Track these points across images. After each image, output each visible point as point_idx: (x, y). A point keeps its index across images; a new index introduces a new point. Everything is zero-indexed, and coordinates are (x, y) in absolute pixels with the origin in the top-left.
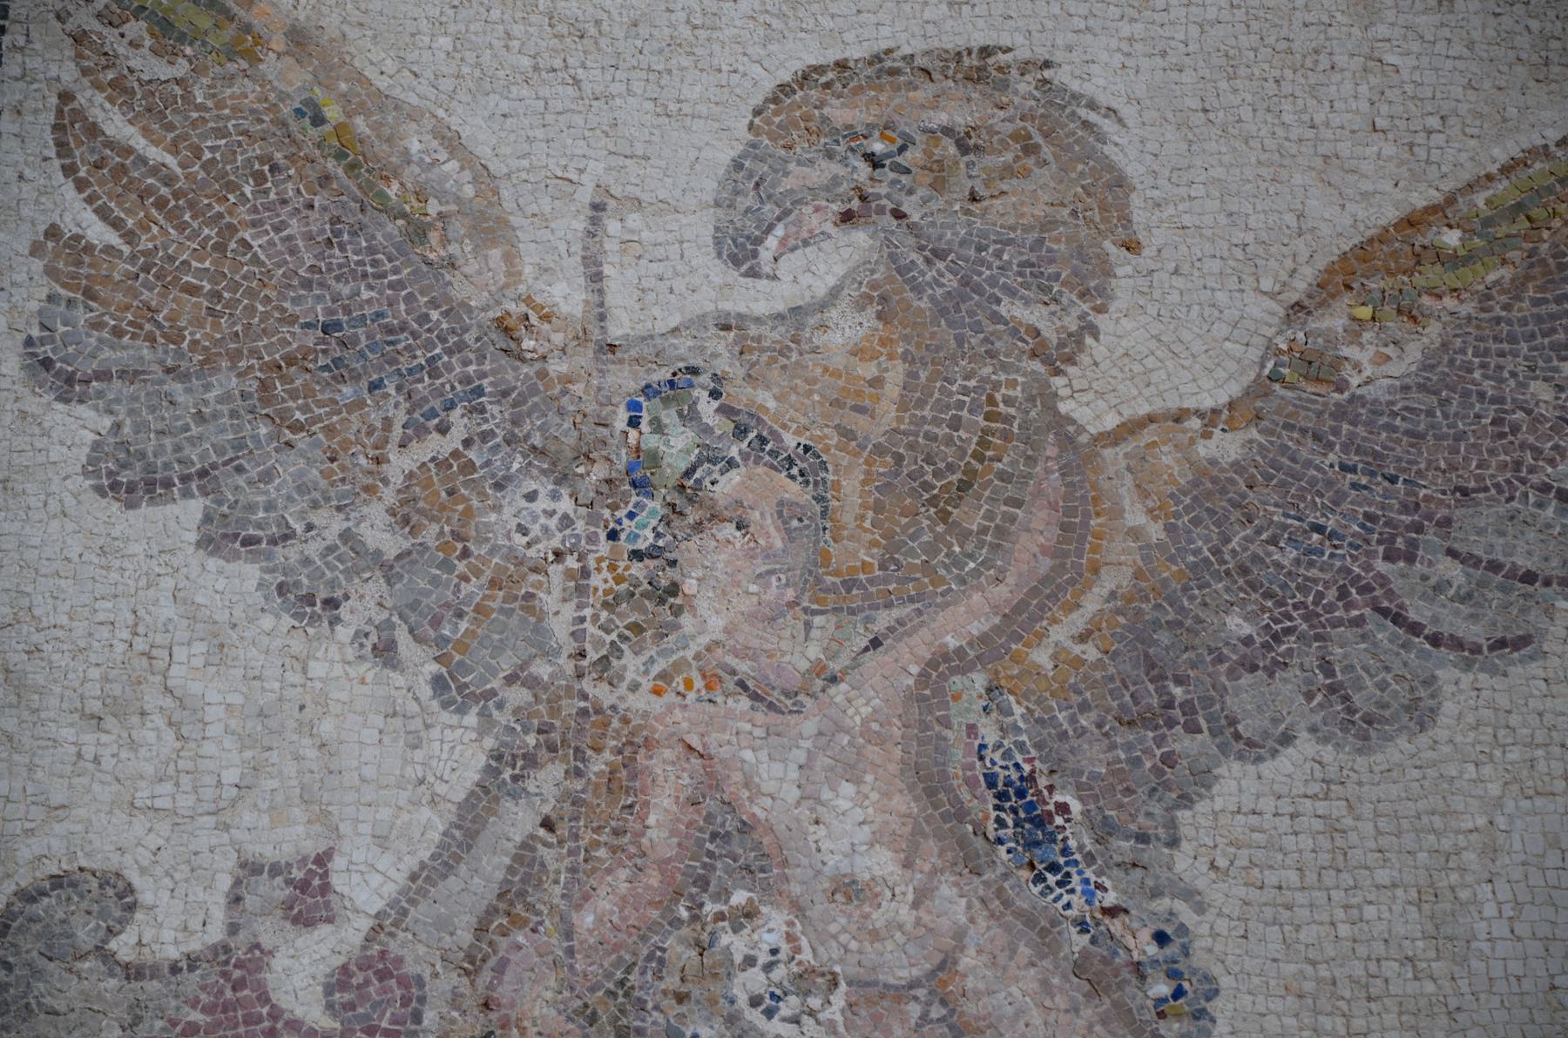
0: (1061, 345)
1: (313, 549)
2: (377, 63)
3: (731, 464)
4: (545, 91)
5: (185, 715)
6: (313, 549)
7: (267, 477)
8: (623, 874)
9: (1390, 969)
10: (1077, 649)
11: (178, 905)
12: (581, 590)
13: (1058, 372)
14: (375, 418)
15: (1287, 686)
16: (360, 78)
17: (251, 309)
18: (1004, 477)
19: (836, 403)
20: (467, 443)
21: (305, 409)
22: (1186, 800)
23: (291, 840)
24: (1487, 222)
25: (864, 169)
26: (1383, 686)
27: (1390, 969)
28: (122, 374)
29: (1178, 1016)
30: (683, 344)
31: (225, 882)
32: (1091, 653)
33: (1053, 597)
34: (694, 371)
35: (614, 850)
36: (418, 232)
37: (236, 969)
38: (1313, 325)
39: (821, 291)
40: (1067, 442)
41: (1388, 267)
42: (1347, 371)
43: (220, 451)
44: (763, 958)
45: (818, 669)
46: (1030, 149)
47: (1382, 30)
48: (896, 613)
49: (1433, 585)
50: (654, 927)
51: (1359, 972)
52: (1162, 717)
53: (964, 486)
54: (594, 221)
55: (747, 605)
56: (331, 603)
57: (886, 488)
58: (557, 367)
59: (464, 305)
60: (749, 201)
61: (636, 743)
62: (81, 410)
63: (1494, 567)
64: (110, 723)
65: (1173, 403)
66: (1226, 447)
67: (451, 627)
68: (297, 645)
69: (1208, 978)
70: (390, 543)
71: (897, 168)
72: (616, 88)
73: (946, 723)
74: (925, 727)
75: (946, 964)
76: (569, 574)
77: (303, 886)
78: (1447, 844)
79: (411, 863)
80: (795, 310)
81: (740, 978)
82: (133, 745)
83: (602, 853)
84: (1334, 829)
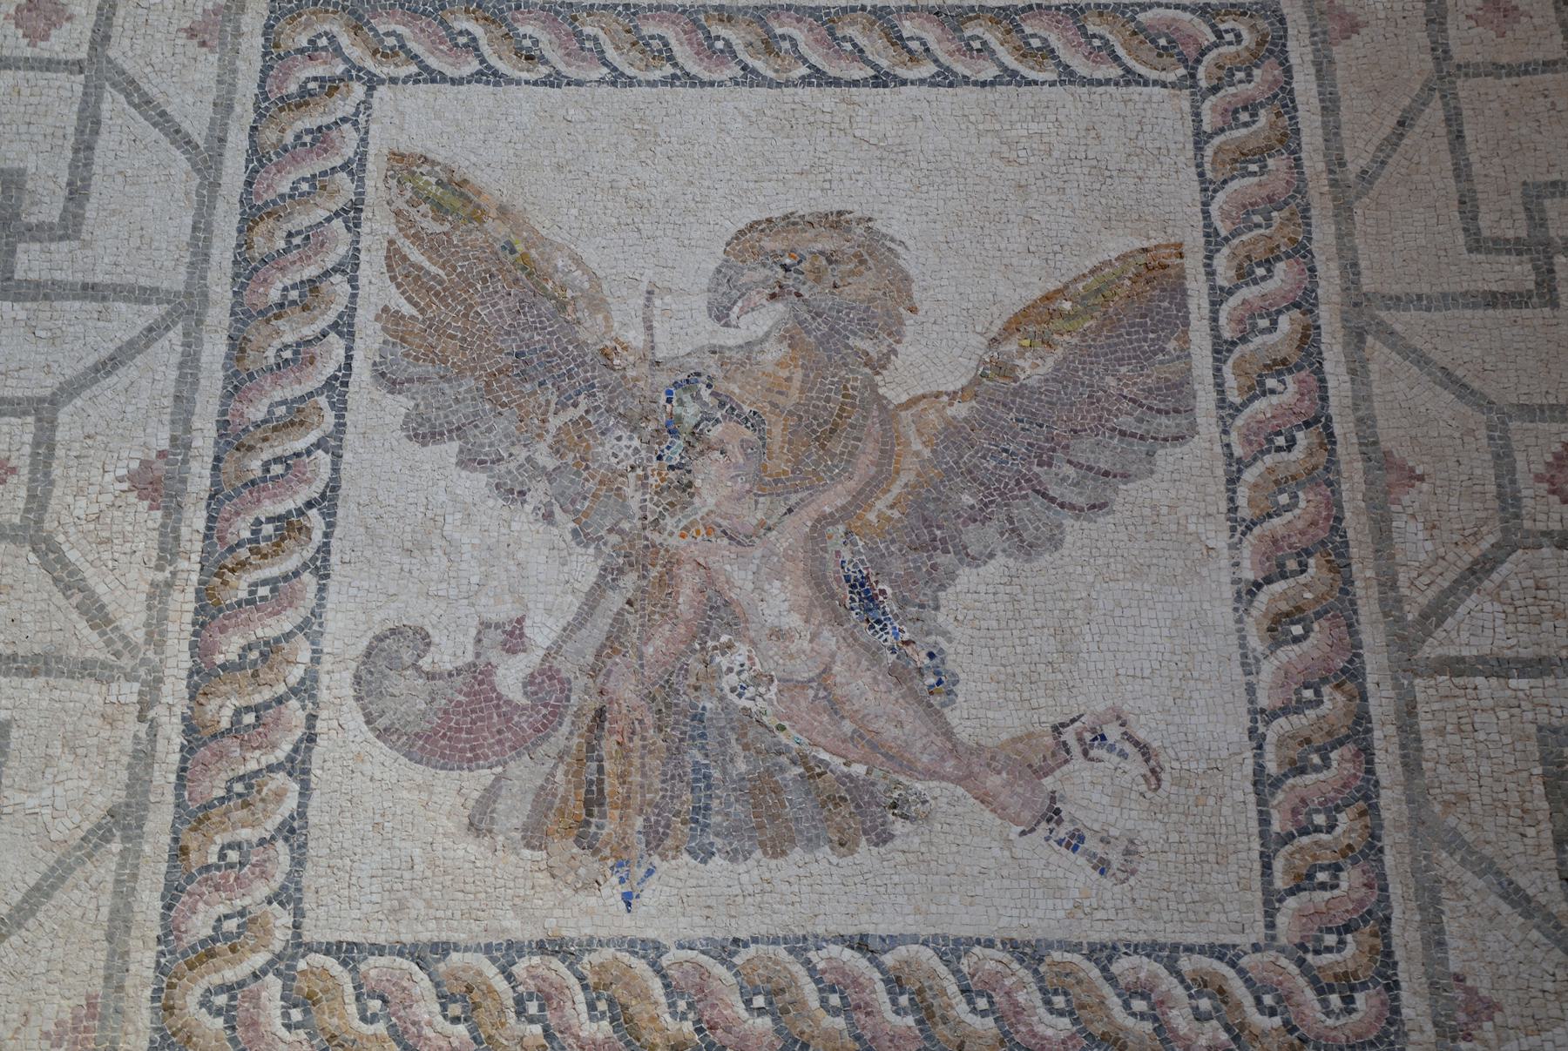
0: (879, 359)
1: (513, 466)
2: (541, 222)
3: (717, 421)
4: (623, 235)
5: (452, 549)
6: (513, 466)
7: (489, 430)
8: (667, 627)
9: (1041, 668)
10: (889, 512)
11: (451, 643)
12: (644, 486)
13: (878, 373)
14: (542, 400)
15: (991, 530)
16: (533, 230)
17: (481, 346)
18: (852, 426)
19: (769, 390)
20: (587, 412)
21: (508, 396)
22: (942, 587)
23: (505, 611)
24: (1084, 298)
25: (781, 272)
26: (1037, 528)
27: (1041, 668)
28: (419, 379)
29: (940, 693)
30: (693, 361)
31: (473, 632)
32: (896, 514)
33: (877, 486)
34: (698, 374)
35: (662, 615)
36: (562, 306)
37: (479, 676)
38: (1001, 349)
39: (761, 334)
40: (883, 408)
41: (1038, 320)
42: (1018, 372)
43: (466, 417)
44: (737, 668)
45: (762, 524)
46: (862, 262)
47: (1031, 203)
48: (800, 495)
49: (1061, 478)
50: (683, 653)
51: (1026, 670)
52: (931, 546)
53: (832, 431)
54: (648, 299)
55: (726, 492)
56: (522, 493)
57: (793, 433)
58: (631, 373)
59: (585, 342)
60: (724, 289)
61: (672, 563)
62: (400, 398)
63: (1090, 469)
64: (416, 553)
65: (934, 389)
66: (960, 410)
67: (581, 505)
68: (506, 514)
69: (954, 675)
71: (797, 271)
72: (659, 233)
73: (825, 550)
74: (815, 552)
75: (827, 670)
76: (638, 477)
77: (511, 634)
78: (1068, 606)
79: (563, 623)
80: (748, 343)
81: (725, 678)
82: (427, 564)
83: (656, 617)
84: (1014, 599)
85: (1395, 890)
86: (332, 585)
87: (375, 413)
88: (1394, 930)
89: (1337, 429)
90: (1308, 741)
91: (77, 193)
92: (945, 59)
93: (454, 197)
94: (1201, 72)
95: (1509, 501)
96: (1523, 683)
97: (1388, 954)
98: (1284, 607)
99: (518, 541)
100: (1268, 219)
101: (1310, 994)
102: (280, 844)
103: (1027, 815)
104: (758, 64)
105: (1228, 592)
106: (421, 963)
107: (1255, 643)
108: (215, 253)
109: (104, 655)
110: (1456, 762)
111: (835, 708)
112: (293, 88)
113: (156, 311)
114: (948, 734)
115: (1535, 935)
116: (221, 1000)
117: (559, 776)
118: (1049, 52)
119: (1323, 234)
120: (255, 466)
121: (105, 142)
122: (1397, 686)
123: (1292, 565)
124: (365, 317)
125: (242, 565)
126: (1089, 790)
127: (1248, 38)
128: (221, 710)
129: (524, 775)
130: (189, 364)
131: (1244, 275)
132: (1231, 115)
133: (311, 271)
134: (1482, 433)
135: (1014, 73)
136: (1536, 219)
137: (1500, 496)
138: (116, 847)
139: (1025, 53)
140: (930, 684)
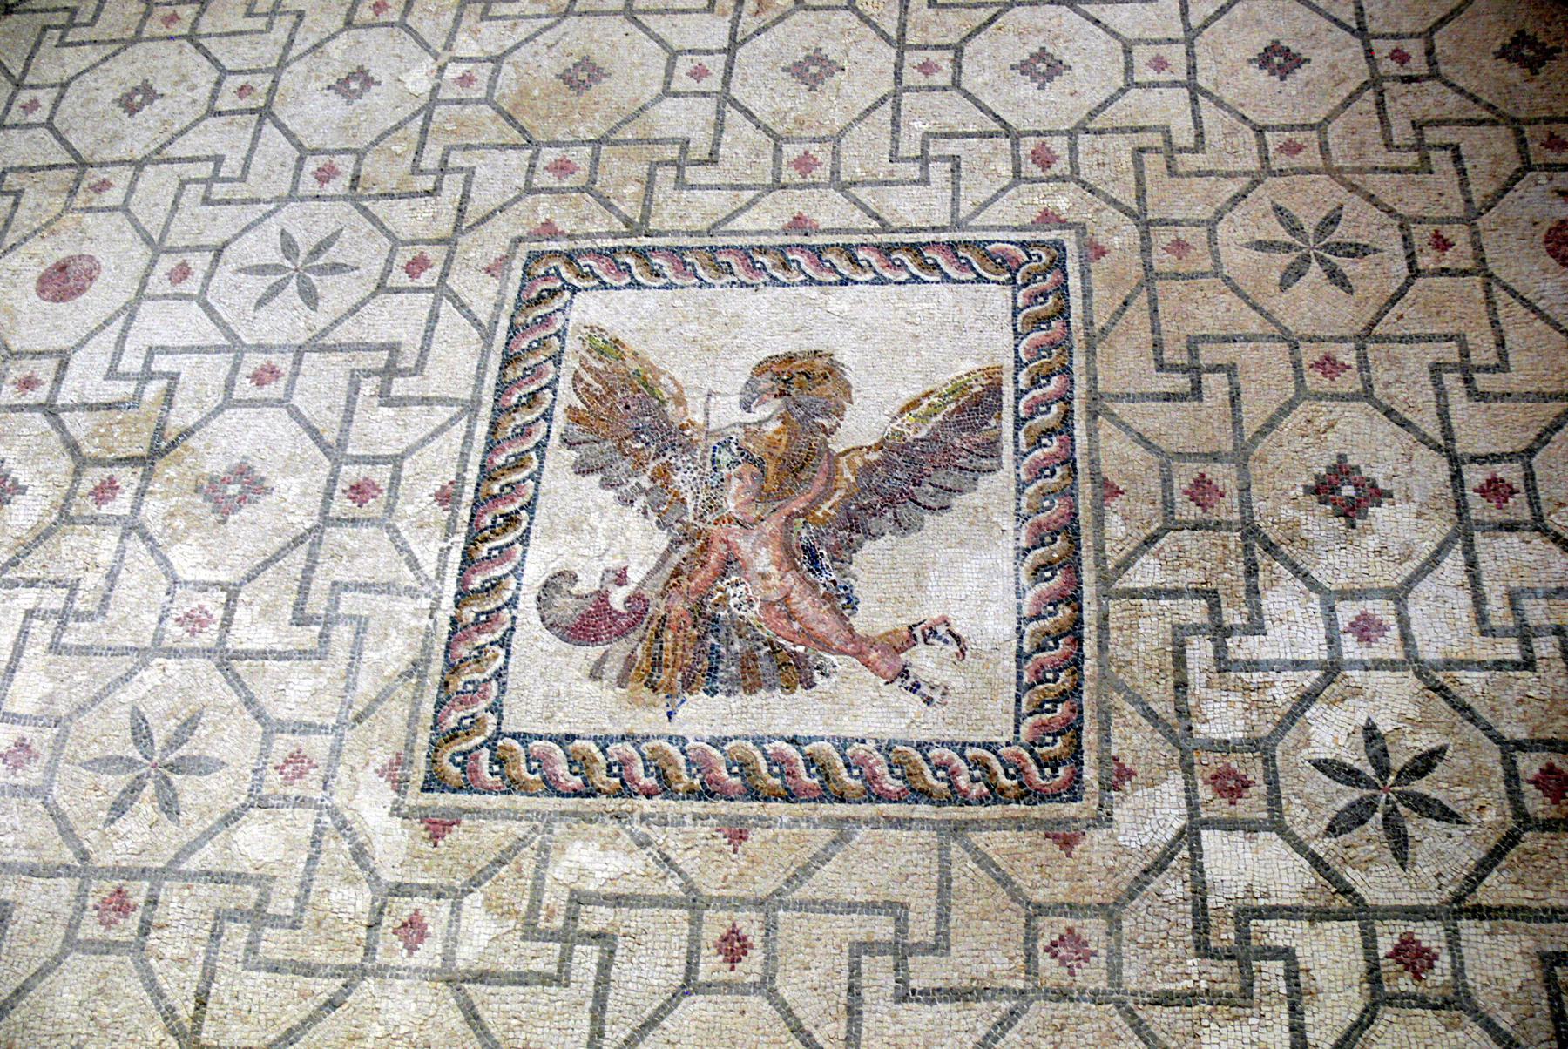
23: (614, 563)
30: (729, 431)
32: (832, 512)
40: (830, 455)
49: (925, 492)
66: (874, 456)
67: (663, 504)
70: (647, 484)
75: (787, 596)
85: (1087, 713)
86: (530, 551)
87: (560, 459)
88: (1084, 733)
89: (1079, 466)
90: (1048, 634)
91: (424, 351)
92: (879, 270)
93: (611, 348)
94: (1019, 277)
95: (1168, 505)
96: (1167, 602)
97: (1079, 746)
98: (1042, 562)
99: (627, 527)
100: (1050, 354)
101: (1034, 768)
102: (494, 683)
103: (890, 674)
104: (778, 274)
105: (1012, 554)
106: (560, 744)
107: (1024, 581)
108: (487, 380)
109: (416, 585)
110: (1127, 645)
111: (790, 616)
112: (534, 295)
113: (455, 409)
114: (851, 630)
115: (1158, 735)
116: (459, 759)
117: (639, 652)
118: (936, 266)
119: (1079, 360)
120: (496, 489)
121: (440, 326)
122: (1100, 604)
123: (1048, 539)
124: (559, 411)
125: (486, 540)
126: (925, 661)
127: (1045, 258)
128: (468, 615)
129: (620, 649)
130: (469, 435)
131: (1034, 383)
132: (1033, 299)
133: (533, 388)
134: (1156, 468)
135: (917, 277)
136: (1194, 354)
137: (1164, 502)
138: (414, 681)
139: (924, 266)
140: (843, 601)
